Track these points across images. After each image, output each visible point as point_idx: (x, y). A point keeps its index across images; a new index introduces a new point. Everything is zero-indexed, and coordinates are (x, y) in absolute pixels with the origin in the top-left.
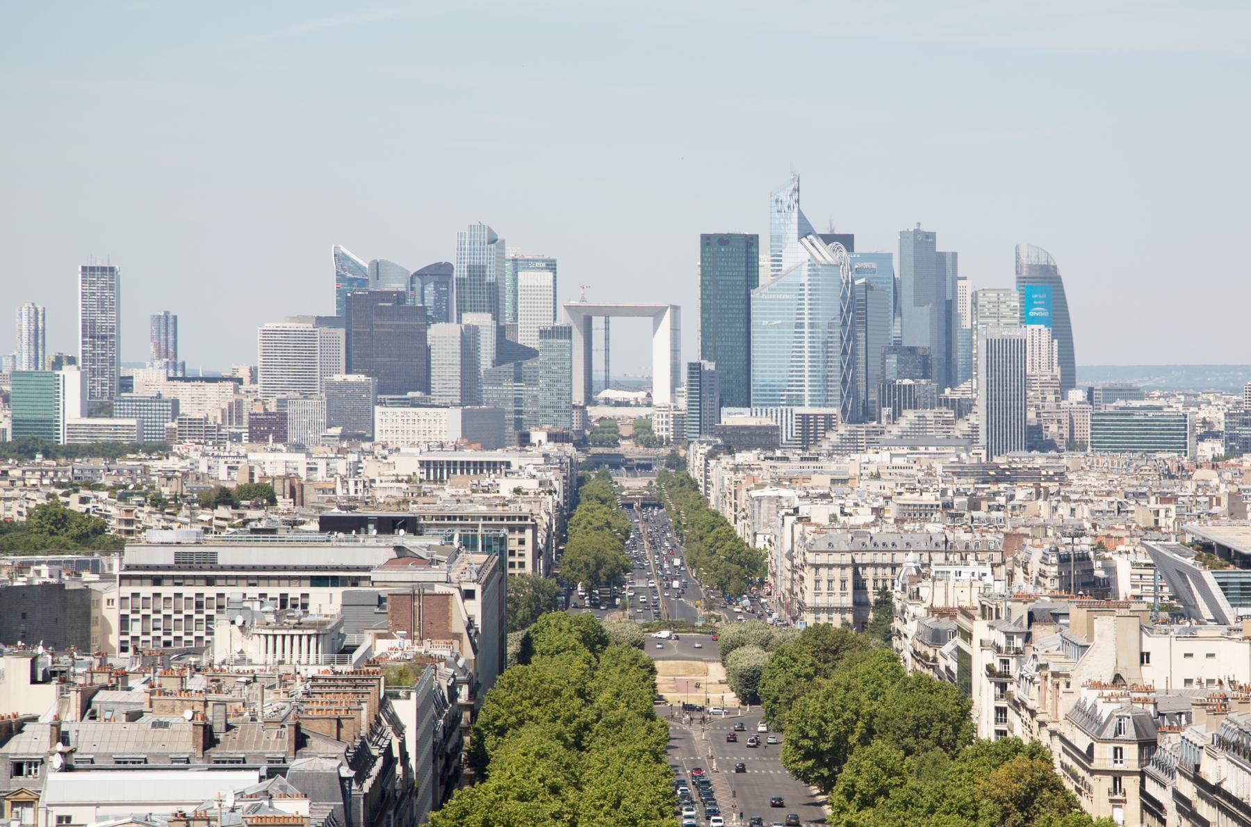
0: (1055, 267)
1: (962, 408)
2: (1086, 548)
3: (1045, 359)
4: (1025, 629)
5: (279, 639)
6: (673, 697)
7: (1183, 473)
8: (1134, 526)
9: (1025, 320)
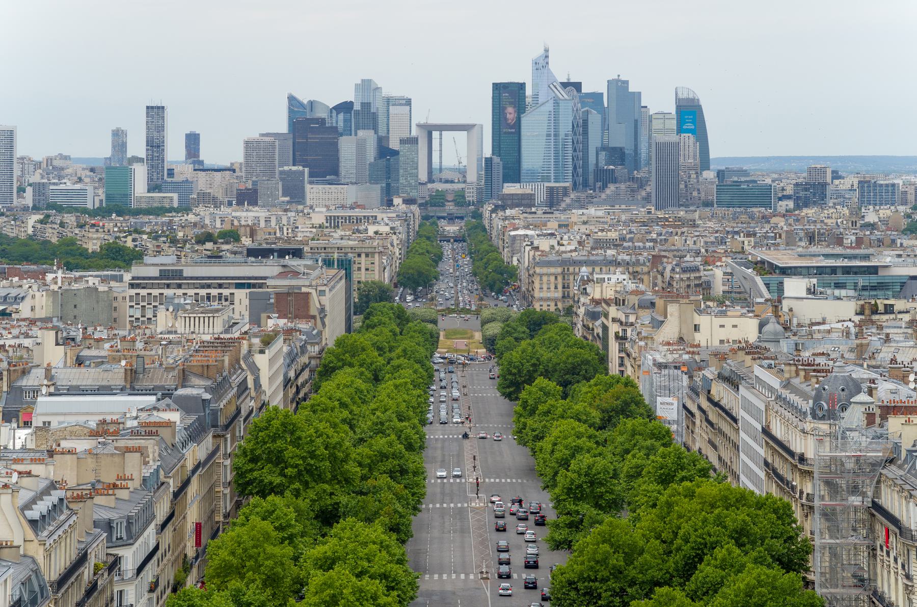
0: (698, 100)
3: (691, 154)
5: (192, 319)
7: (766, 219)
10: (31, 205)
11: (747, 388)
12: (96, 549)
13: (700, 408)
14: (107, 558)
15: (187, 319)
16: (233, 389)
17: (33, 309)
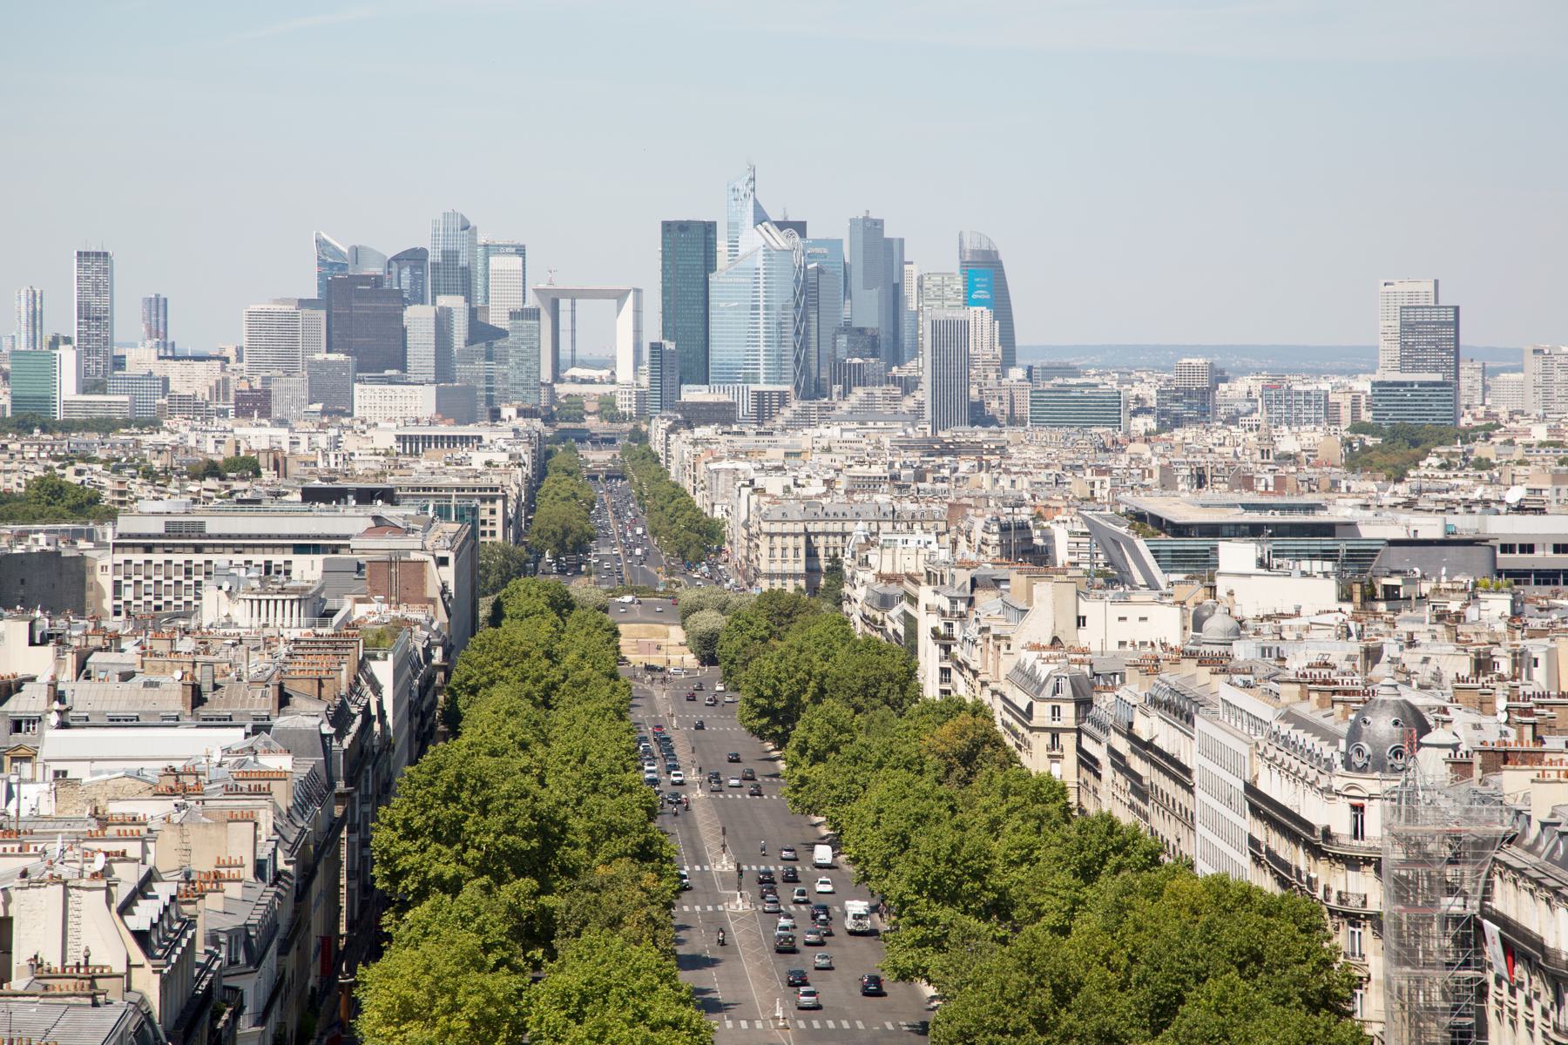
1: (909, 386)
2: (1025, 517)
4: (968, 594)
5: (263, 603)
6: (636, 658)
7: (1117, 447)
8: (1071, 496)
9: (968, 302)
15: (255, 603)
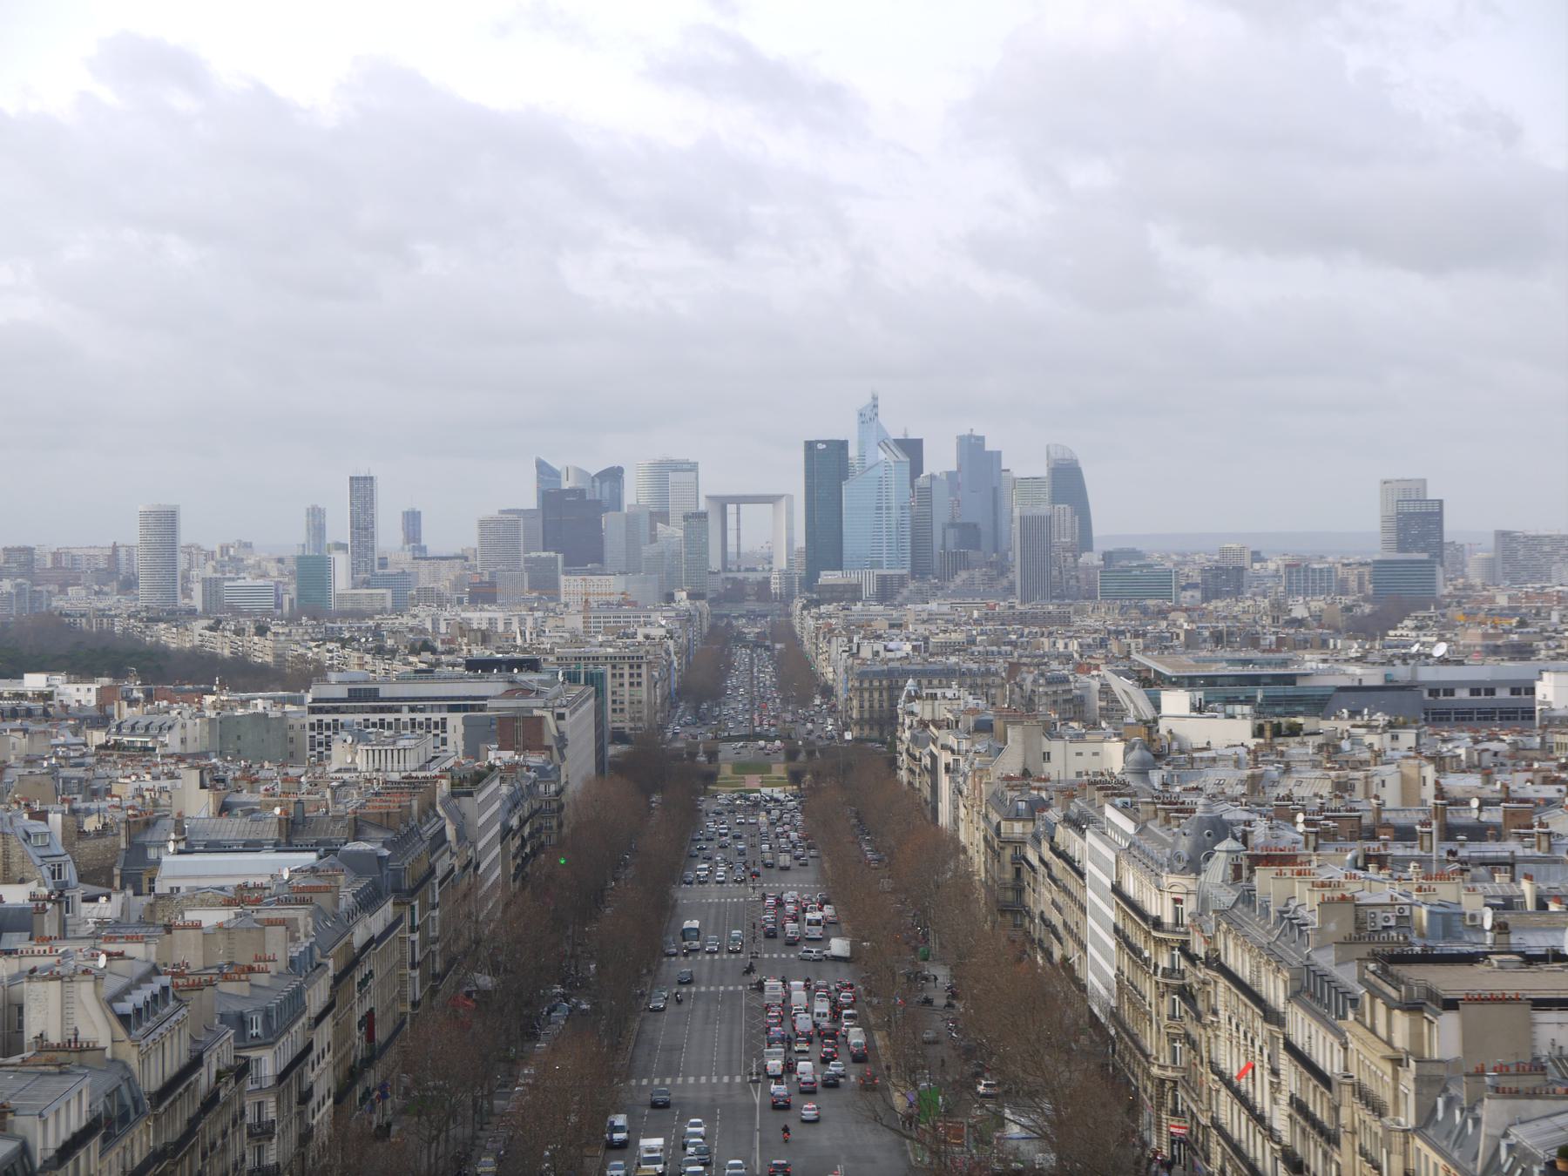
0: (1077, 461)
5: (377, 753)
7: (1162, 614)
8: (1110, 655)
10: (200, 608)
11: (1095, 833)
12: (219, 1050)
13: (1041, 860)
14: (236, 1062)
16: (424, 842)
17: (183, 741)
